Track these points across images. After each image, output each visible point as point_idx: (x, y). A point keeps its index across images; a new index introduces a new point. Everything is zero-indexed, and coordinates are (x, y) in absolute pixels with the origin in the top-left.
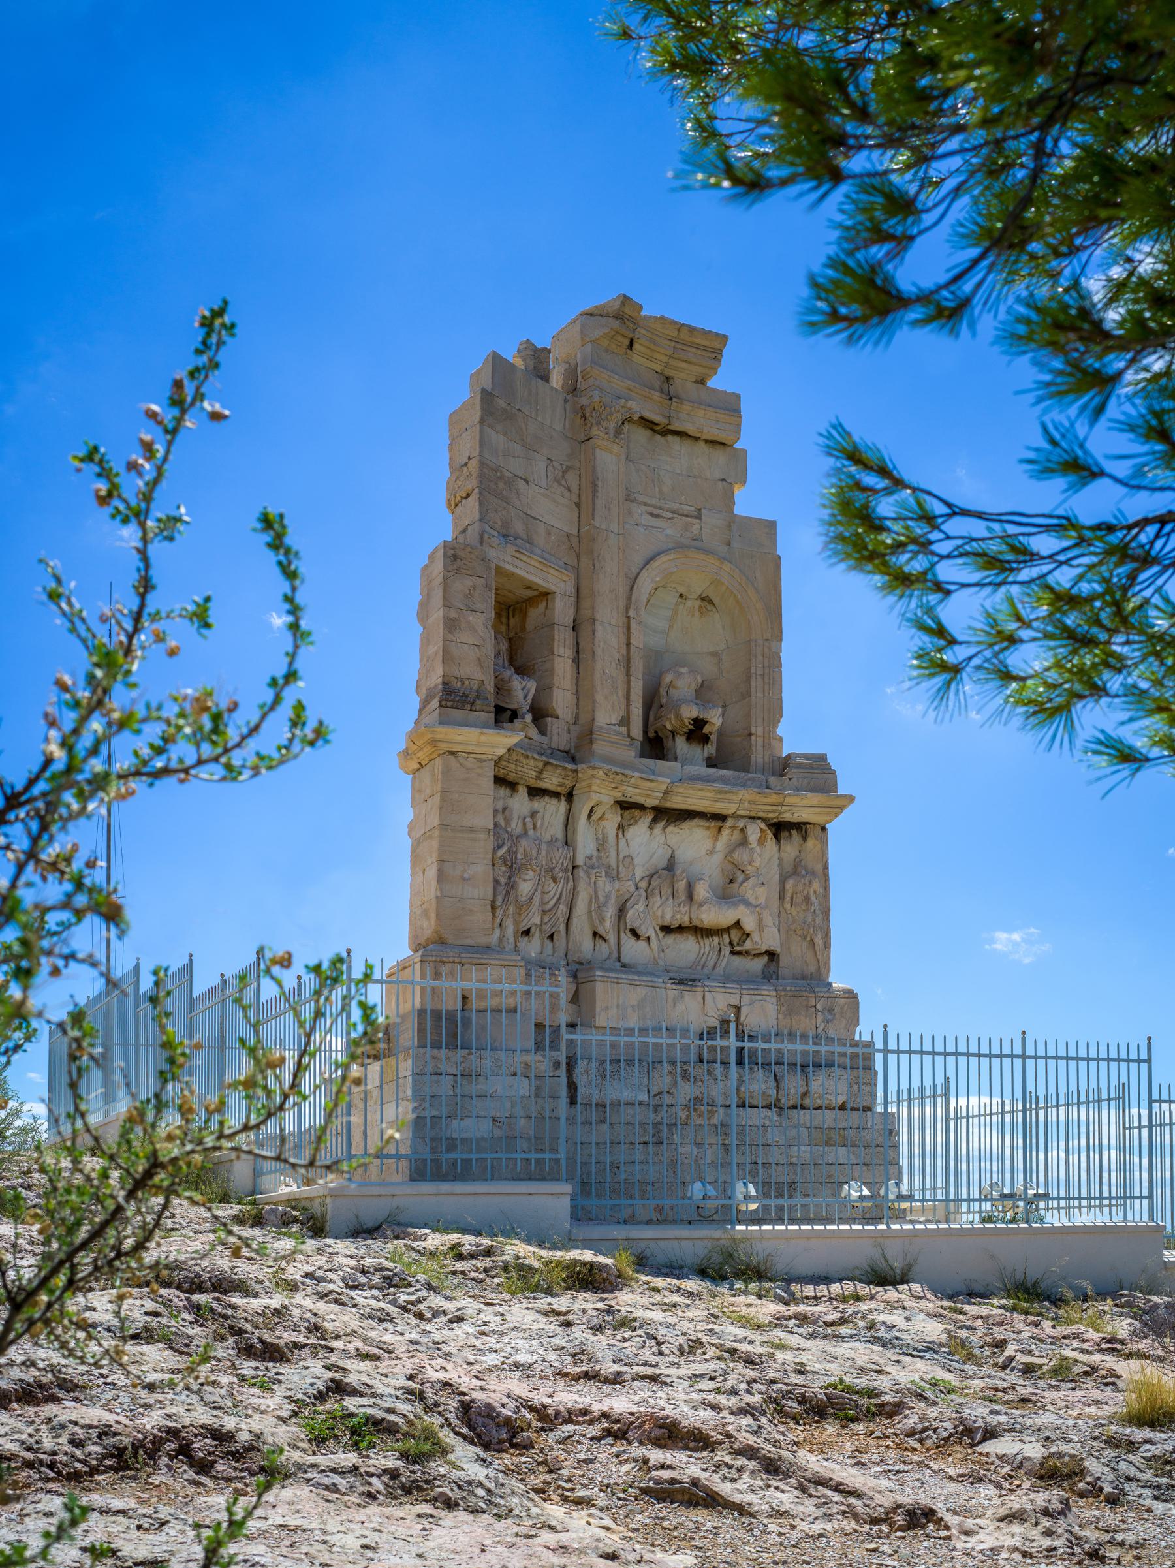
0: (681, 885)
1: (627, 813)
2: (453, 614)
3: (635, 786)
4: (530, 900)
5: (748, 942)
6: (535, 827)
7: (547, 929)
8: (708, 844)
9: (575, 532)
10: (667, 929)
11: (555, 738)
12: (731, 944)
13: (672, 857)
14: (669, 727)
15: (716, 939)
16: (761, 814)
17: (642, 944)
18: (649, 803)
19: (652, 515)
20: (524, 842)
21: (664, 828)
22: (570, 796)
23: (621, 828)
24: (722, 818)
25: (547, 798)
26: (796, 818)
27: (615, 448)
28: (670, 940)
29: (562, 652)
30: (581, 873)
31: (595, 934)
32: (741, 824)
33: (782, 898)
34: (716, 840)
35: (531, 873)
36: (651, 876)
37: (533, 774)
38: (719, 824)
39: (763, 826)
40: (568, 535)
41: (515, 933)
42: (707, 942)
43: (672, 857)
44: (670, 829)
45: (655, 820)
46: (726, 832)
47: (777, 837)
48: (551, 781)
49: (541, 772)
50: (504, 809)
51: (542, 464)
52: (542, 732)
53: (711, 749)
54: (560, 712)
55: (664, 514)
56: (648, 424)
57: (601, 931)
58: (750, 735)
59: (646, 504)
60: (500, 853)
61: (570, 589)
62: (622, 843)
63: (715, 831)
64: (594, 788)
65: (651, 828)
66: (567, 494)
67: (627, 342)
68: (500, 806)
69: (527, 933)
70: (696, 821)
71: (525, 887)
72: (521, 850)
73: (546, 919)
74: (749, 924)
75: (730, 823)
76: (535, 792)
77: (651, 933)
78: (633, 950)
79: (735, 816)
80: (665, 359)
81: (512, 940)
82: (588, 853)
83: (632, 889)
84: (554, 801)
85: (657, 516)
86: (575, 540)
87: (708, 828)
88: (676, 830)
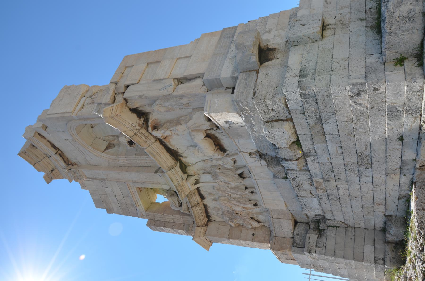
1: (187, 165)
3: (177, 180)
19: (84, 154)
25: (202, 193)
26: (135, 116)
27: (81, 172)
37: (198, 208)
39: (150, 129)
49: (196, 205)
63: (167, 139)
64: (189, 191)
67: (53, 172)
68: (215, 213)
70: (170, 146)
76: (202, 197)
80: (44, 160)
87: (169, 142)
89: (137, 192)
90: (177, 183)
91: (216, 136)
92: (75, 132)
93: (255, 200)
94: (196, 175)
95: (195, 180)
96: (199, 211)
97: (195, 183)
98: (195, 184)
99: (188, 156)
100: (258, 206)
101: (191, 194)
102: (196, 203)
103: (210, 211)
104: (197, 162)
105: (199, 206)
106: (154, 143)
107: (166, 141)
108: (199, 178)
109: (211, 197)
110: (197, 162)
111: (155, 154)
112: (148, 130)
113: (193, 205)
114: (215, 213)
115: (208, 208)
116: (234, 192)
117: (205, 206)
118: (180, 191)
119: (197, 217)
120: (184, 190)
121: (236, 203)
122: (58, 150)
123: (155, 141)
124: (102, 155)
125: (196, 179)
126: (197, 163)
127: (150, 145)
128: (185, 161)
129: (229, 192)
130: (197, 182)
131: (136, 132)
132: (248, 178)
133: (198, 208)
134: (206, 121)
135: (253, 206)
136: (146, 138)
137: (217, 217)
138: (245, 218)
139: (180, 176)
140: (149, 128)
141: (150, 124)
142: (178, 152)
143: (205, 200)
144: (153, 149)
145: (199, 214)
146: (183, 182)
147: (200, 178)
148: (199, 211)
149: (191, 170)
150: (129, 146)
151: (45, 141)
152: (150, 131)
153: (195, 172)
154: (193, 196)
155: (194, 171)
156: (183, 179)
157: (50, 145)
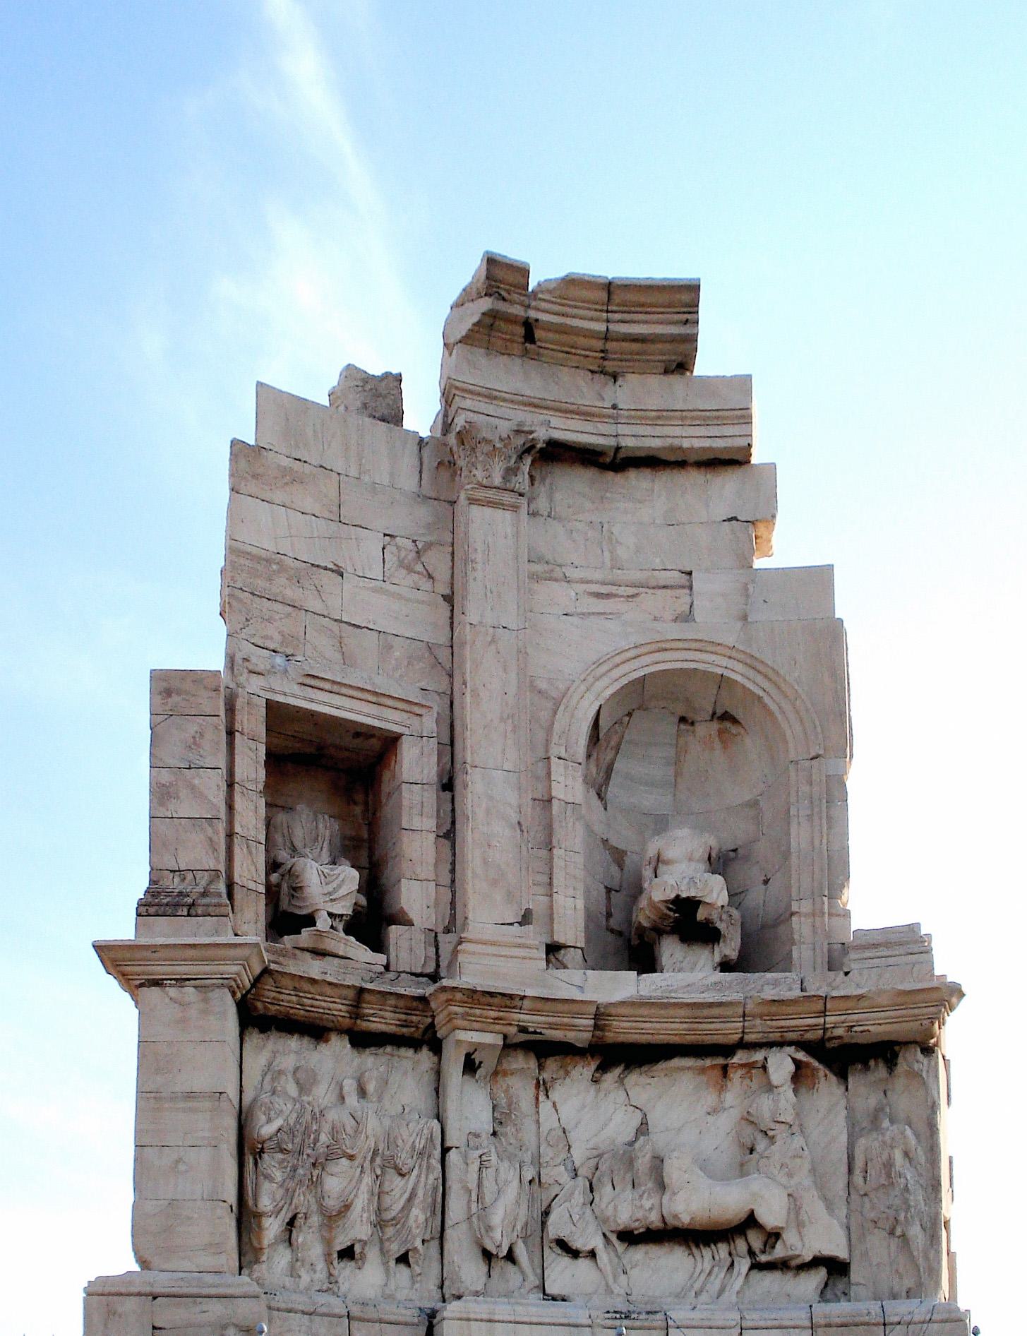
0: (643, 1163)
1: (552, 1064)
2: (166, 776)
4: (347, 1207)
5: (779, 1246)
6: (362, 1093)
7: (396, 1249)
8: (710, 1099)
9: (443, 638)
10: (629, 1237)
11: (404, 955)
12: (751, 1253)
13: (644, 1123)
14: (645, 924)
15: (723, 1249)
16: (791, 1036)
17: (583, 1263)
18: (580, 1037)
20: (332, 1115)
21: (621, 1081)
22: (436, 1047)
23: (542, 1087)
24: (726, 1050)
25: (389, 1049)
28: (639, 1254)
29: (416, 824)
30: (453, 1156)
31: (487, 1256)
32: (758, 1056)
33: (850, 1171)
34: (722, 1089)
35: (344, 1161)
36: (600, 1156)
38: (720, 1061)
39: (801, 1056)
40: (429, 647)
41: (328, 1255)
42: (707, 1252)
43: (644, 1123)
44: (635, 1079)
45: (603, 1068)
46: (736, 1076)
47: (843, 1076)
48: (381, 1020)
50: (297, 1069)
51: (372, 544)
52: (378, 945)
53: (730, 948)
54: (413, 915)
55: (622, 591)
56: (587, 457)
57: (491, 1248)
58: (792, 914)
59: (583, 581)
60: (267, 1130)
61: (429, 724)
62: (545, 1106)
63: (717, 1073)
65: (595, 1081)
66: (426, 585)
68: (288, 1062)
69: (347, 1254)
70: (677, 1062)
71: (336, 1182)
72: (326, 1128)
73: (390, 1231)
74: (770, 1217)
75: (740, 1057)
76: (363, 1040)
77: (597, 1242)
78: (562, 1273)
79: (742, 1045)
81: (321, 1265)
82: (474, 1126)
83: (565, 1178)
84: (408, 1053)
85: (608, 596)
86: (444, 655)
87: (703, 1070)
88: (644, 1080)
89: (377, 723)
90: (524, 1007)
91: (720, 1245)
92: (738, 678)
93: (363, 1256)
94: (496, 1073)
95: (481, 1063)
96: (323, 1004)
97: (473, 1057)
98: (468, 1056)
99: (598, 1091)
100: (335, 1262)
101: (418, 1013)
102: (367, 1011)
103: (294, 1043)
104: (554, 1104)
105: (347, 1015)
106: (740, 1036)
107: (713, 1067)
108: (477, 1076)
109: (374, 1083)
110: (554, 1104)
111: (698, 1013)
112: (801, 1045)
113: (367, 996)
114: (288, 1062)
115: (306, 1040)
116: (420, 1193)
117: (316, 1031)
118: (483, 1000)
119: (306, 986)
120: (478, 1012)
121: (368, 1184)
122: (618, 461)
123: (742, 1038)
124: (590, 697)
125: (479, 1066)
126: (549, 1104)
127: (744, 1021)
128: (579, 1068)
129: (419, 1176)
130: (470, 1066)
131: (828, 1019)
132: (485, 1269)
133: (340, 1007)
134: (818, 1254)
135: (349, 1244)
136: (782, 1028)
137: (263, 1059)
138: (302, 1198)
139: (544, 1031)
140: (804, 1053)
141: (816, 1064)
142: (627, 1068)
143: (349, 1046)
144: (723, 1019)
145: (312, 999)
146: (511, 1024)
147: (477, 1081)
148: (323, 1004)
149: (523, 1063)
150: (684, 895)
151: (692, 458)
152: (791, 1050)
153: (505, 1074)
154: (403, 1017)
155: (512, 1074)
156: (523, 1030)
157: (664, 458)
